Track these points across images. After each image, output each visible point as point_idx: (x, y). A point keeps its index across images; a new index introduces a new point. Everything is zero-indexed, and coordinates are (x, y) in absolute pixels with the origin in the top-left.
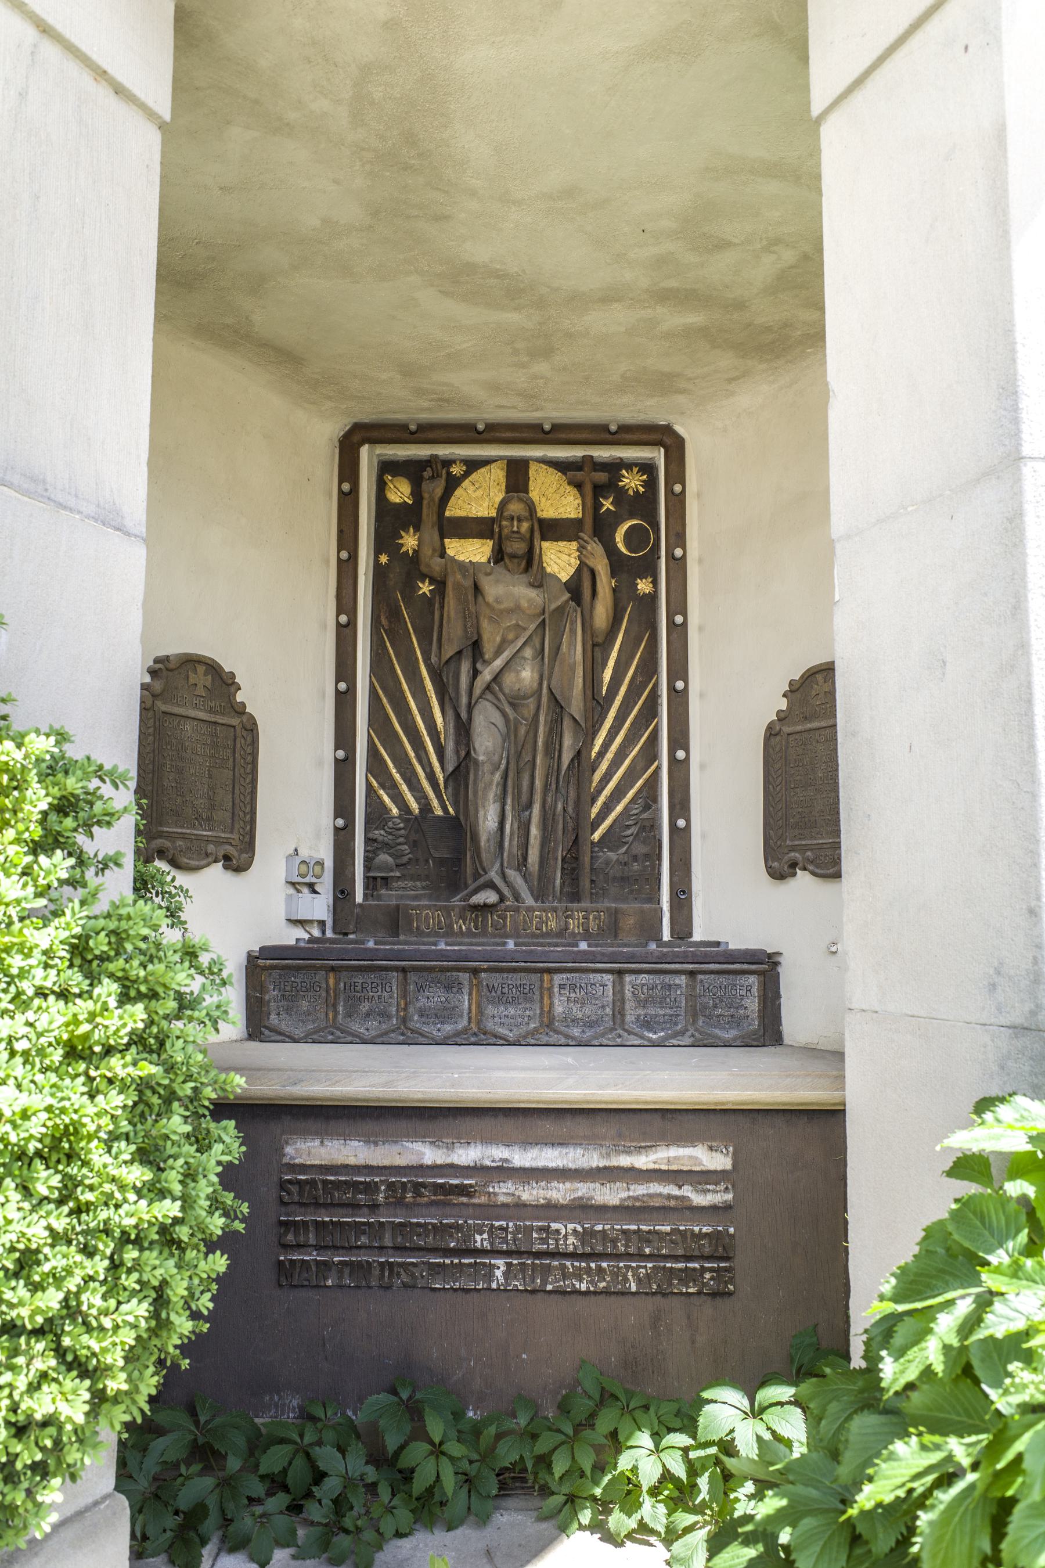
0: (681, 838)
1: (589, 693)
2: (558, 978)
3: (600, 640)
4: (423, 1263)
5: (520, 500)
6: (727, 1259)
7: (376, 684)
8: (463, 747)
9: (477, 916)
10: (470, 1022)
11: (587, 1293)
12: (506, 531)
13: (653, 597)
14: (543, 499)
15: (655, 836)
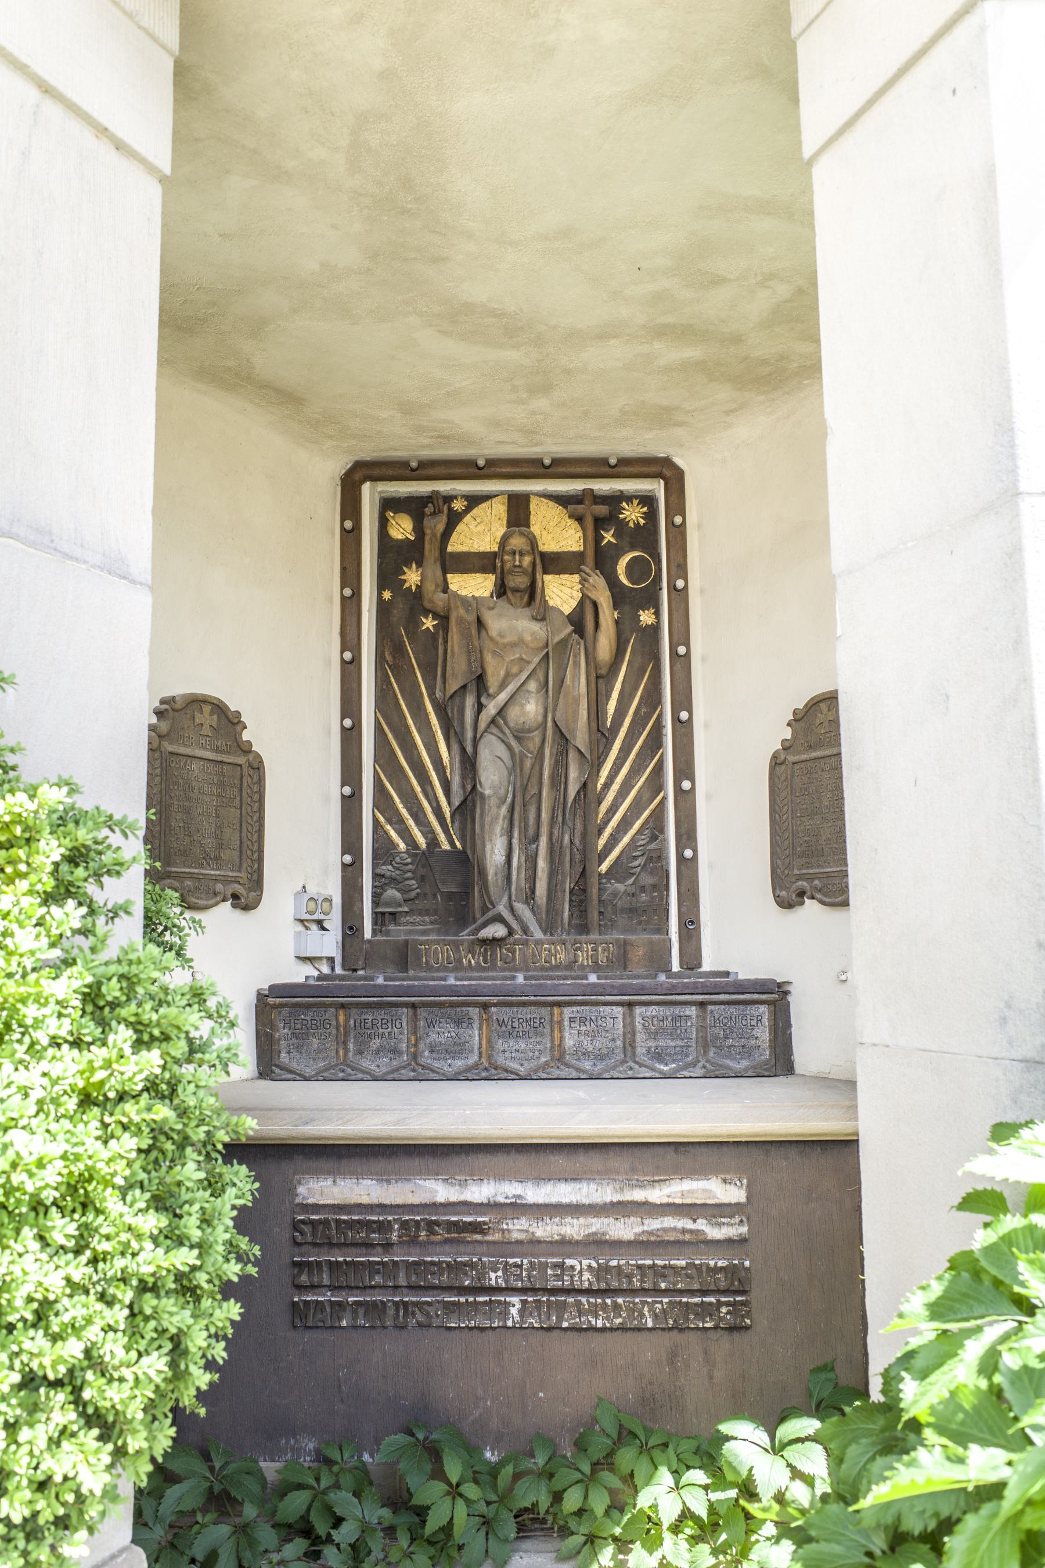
0: (688, 867)
1: (594, 725)
2: (568, 1012)
3: (603, 672)
4: (438, 1302)
5: (522, 534)
7: (381, 720)
8: (469, 781)
9: (486, 950)
10: (480, 1057)
11: (604, 1329)
12: (508, 566)
13: (656, 628)
14: (545, 533)
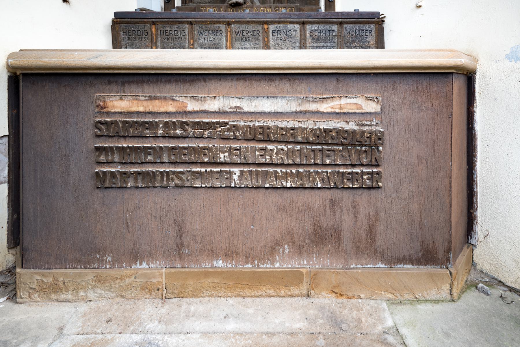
4: (188, 171)
6: (378, 166)
11: (291, 188)
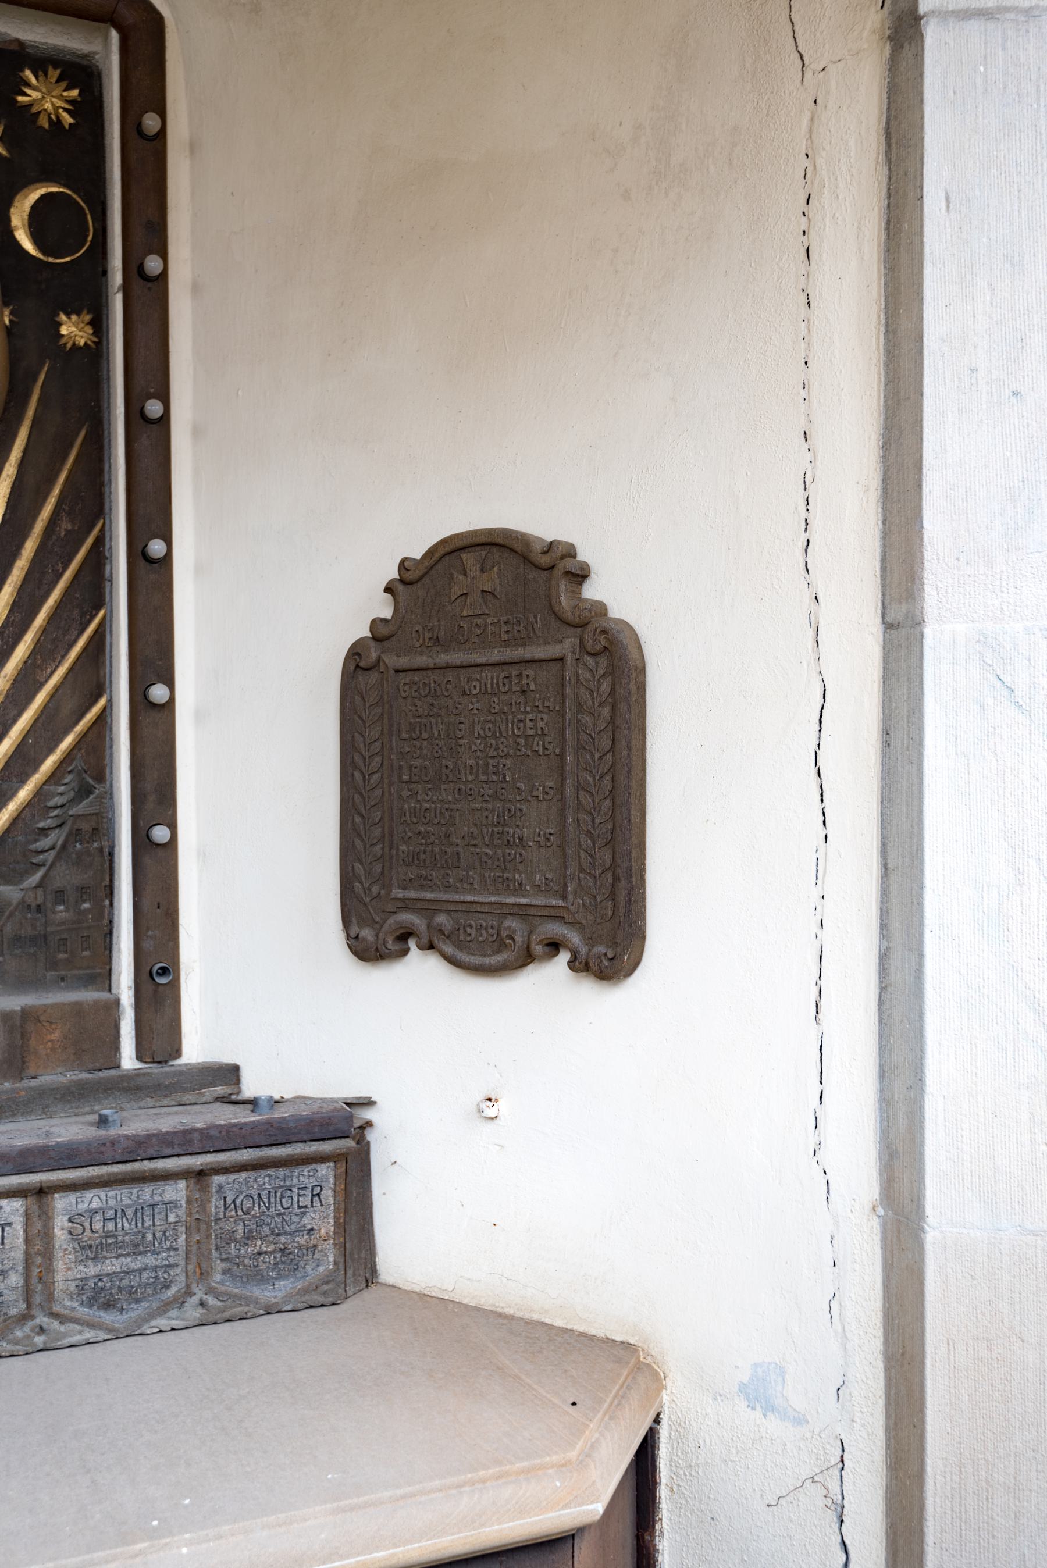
0: (157, 863)
13: (95, 354)
15: (101, 850)
